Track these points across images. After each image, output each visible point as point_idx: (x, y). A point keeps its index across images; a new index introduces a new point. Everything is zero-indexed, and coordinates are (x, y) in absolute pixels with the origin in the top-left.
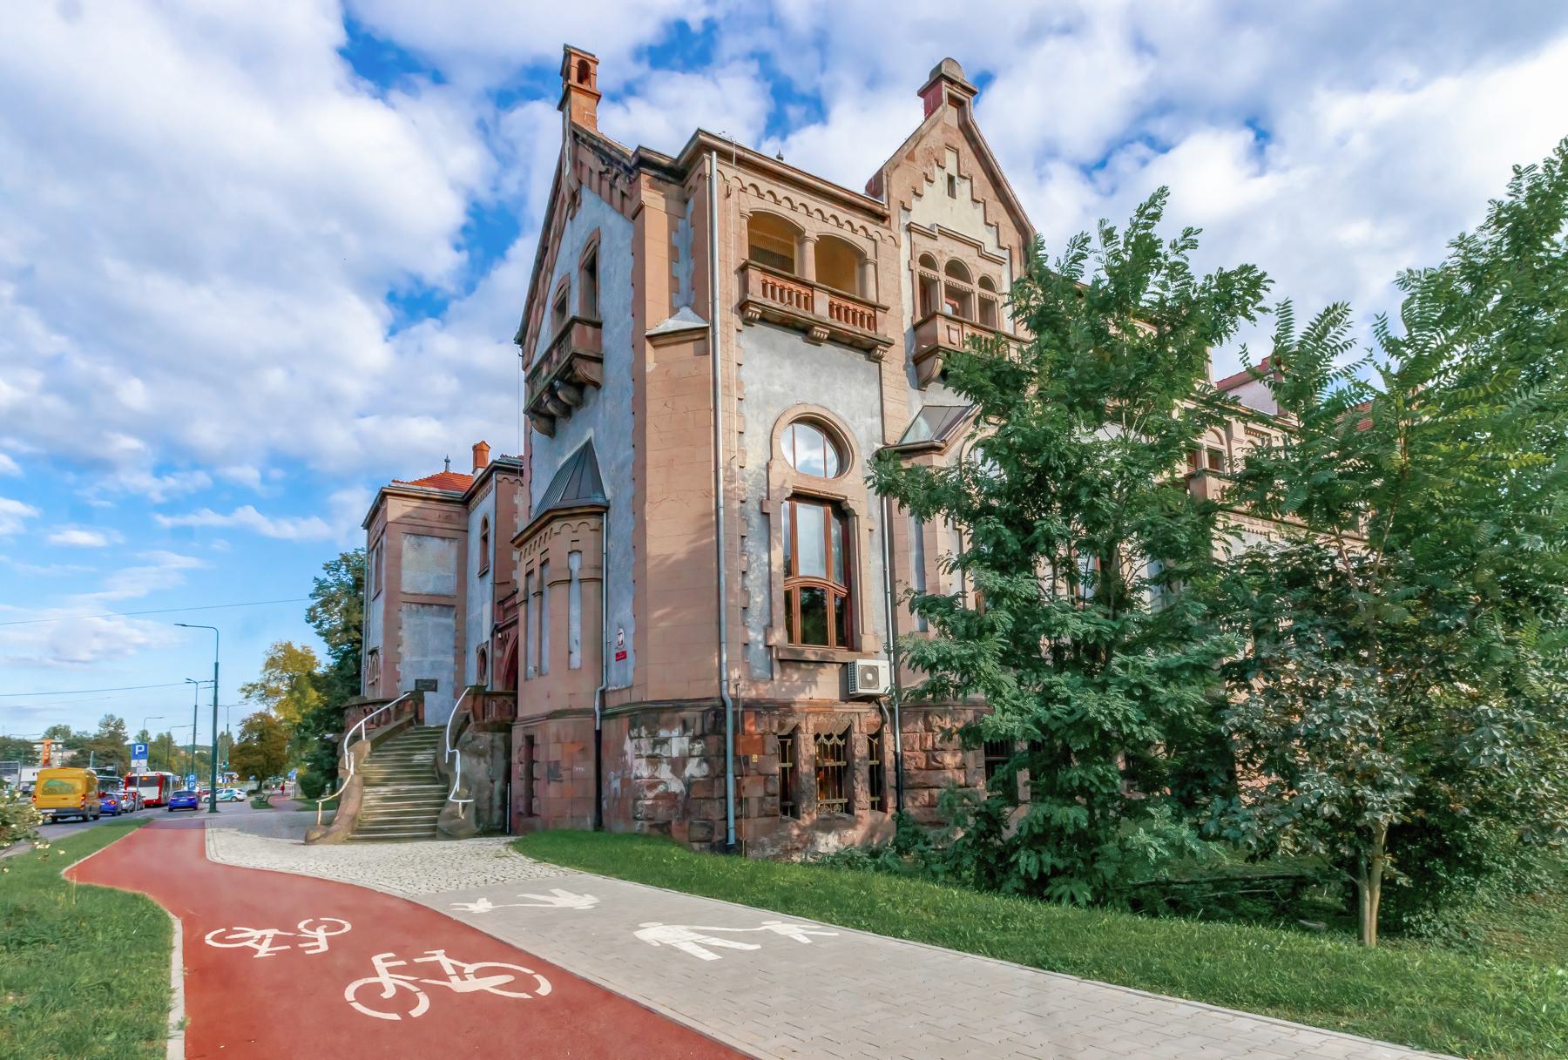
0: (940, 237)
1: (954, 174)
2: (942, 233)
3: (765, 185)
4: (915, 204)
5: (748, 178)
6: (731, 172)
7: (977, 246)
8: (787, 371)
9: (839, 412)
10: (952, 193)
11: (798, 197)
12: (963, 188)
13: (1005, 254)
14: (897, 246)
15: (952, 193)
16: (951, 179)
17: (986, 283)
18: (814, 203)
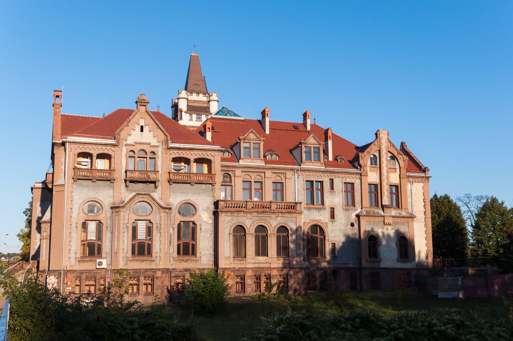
0: (136, 145)
1: (143, 125)
2: (136, 143)
3: (81, 146)
4: (129, 138)
5: (76, 146)
6: (72, 146)
7: (149, 144)
8: (86, 190)
9: (100, 198)
10: (142, 130)
11: (90, 147)
12: (146, 129)
13: (160, 144)
14: (122, 151)
15: (142, 130)
16: (142, 127)
17: (153, 152)
18: (95, 147)
